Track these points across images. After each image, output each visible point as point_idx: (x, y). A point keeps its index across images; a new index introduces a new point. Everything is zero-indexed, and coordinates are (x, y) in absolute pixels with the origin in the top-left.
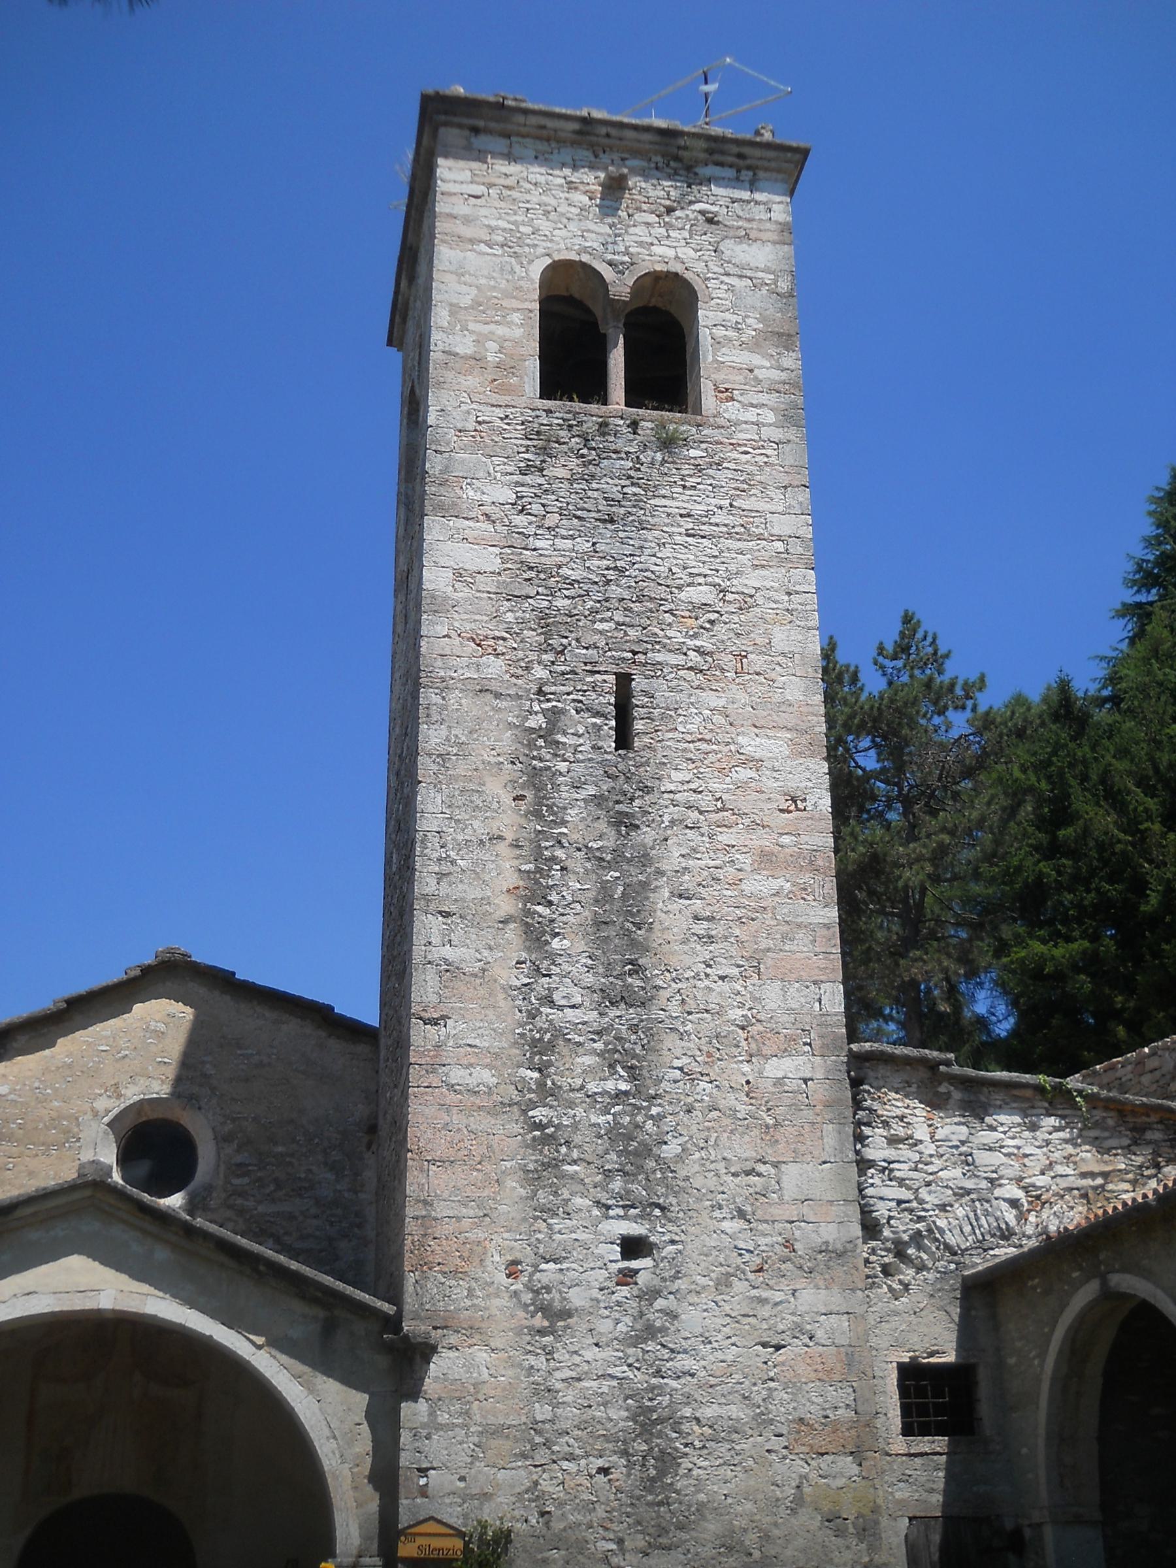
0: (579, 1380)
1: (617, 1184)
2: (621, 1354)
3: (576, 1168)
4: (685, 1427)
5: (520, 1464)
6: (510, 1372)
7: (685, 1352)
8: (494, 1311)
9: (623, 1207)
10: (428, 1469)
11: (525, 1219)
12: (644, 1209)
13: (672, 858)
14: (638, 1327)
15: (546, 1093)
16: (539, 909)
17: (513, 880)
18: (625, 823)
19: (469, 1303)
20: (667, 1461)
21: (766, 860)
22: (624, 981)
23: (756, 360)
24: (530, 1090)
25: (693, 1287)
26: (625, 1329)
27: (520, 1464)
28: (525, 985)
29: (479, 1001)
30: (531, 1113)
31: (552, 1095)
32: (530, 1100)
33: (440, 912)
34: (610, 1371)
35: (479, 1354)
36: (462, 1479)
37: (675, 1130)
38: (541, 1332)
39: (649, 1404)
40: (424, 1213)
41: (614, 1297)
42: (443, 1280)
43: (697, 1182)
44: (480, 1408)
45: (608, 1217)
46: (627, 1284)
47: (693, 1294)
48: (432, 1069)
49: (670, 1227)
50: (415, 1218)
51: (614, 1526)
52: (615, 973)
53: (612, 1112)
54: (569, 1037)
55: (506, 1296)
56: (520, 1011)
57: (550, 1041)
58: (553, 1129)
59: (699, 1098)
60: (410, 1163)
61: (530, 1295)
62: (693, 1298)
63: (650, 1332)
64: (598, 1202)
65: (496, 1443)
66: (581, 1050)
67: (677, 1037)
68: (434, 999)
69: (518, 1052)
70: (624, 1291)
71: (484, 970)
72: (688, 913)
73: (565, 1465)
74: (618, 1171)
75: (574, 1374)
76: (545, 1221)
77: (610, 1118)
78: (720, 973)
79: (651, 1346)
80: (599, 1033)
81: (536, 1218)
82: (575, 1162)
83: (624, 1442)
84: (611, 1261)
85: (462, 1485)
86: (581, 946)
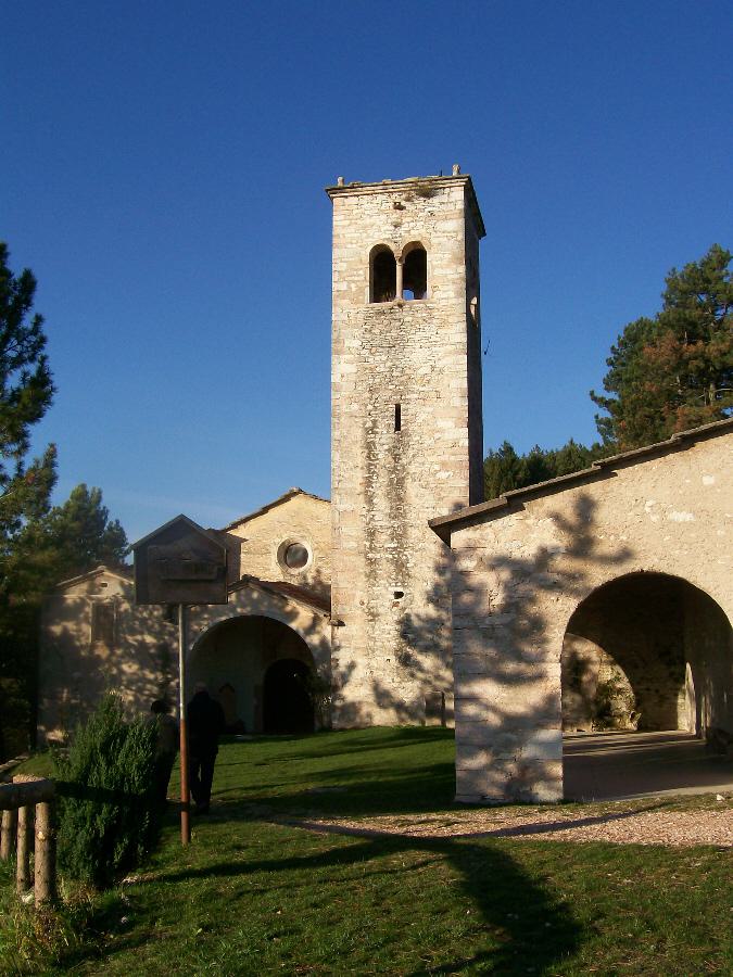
13: (412, 469)
17: (361, 480)
18: (396, 458)
21: (444, 465)
23: (449, 271)
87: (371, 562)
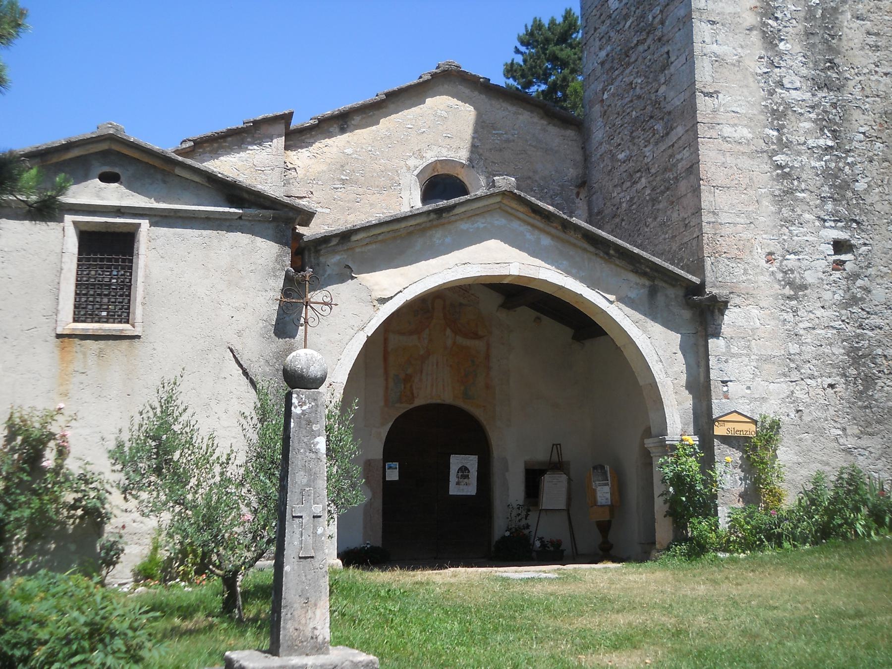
0: (814, 328)
1: (829, 206)
2: (837, 314)
3: (803, 195)
4: (879, 361)
5: (782, 380)
6: (773, 323)
7: (876, 314)
8: (761, 284)
9: (835, 221)
10: (727, 382)
11: (775, 226)
12: (847, 223)
14: (847, 297)
15: (784, 145)
16: (770, 22)
19: (745, 278)
20: (869, 381)
22: (826, 74)
24: (773, 143)
25: (879, 273)
26: (839, 298)
27: (782, 380)
28: (765, 73)
29: (738, 82)
30: (774, 158)
31: (786, 147)
32: (773, 149)
33: (709, 21)
34: (832, 324)
35: (754, 311)
36: (749, 388)
37: (863, 173)
38: (789, 298)
39: (856, 345)
40: (713, 220)
41: (832, 278)
42: (728, 263)
43: (878, 207)
44: (756, 345)
45: (825, 227)
46: (839, 270)
47: (879, 277)
48: (712, 126)
49: (863, 235)
50: (709, 223)
51: (840, 420)
52: (820, 68)
53: (824, 159)
54: (794, 109)
55: (767, 274)
56: (764, 90)
57: (783, 112)
58: (788, 169)
59: (876, 153)
60: (702, 187)
61: (781, 275)
62: (879, 280)
63: (854, 300)
64: (819, 217)
65: (767, 366)
66: (802, 118)
67: (860, 112)
68: (709, 79)
69: (763, 117)
70: (837, 275)
71: (739, 62)
72: (863, 30)
73: (809, 381)
74: (829, 198)
75: (810, 325)
76: (787, 228)
77: (823, 163)
78: (884, 71)
79: (855, 309)
80: (813, 107)
81: (782, 226)
82: (803, 191)
83: (843, 368)
84: (828, 255)
85: (748, 391)
86: (798, 48)
87: (784, 173)
